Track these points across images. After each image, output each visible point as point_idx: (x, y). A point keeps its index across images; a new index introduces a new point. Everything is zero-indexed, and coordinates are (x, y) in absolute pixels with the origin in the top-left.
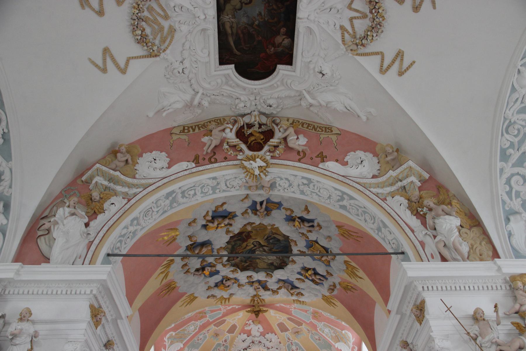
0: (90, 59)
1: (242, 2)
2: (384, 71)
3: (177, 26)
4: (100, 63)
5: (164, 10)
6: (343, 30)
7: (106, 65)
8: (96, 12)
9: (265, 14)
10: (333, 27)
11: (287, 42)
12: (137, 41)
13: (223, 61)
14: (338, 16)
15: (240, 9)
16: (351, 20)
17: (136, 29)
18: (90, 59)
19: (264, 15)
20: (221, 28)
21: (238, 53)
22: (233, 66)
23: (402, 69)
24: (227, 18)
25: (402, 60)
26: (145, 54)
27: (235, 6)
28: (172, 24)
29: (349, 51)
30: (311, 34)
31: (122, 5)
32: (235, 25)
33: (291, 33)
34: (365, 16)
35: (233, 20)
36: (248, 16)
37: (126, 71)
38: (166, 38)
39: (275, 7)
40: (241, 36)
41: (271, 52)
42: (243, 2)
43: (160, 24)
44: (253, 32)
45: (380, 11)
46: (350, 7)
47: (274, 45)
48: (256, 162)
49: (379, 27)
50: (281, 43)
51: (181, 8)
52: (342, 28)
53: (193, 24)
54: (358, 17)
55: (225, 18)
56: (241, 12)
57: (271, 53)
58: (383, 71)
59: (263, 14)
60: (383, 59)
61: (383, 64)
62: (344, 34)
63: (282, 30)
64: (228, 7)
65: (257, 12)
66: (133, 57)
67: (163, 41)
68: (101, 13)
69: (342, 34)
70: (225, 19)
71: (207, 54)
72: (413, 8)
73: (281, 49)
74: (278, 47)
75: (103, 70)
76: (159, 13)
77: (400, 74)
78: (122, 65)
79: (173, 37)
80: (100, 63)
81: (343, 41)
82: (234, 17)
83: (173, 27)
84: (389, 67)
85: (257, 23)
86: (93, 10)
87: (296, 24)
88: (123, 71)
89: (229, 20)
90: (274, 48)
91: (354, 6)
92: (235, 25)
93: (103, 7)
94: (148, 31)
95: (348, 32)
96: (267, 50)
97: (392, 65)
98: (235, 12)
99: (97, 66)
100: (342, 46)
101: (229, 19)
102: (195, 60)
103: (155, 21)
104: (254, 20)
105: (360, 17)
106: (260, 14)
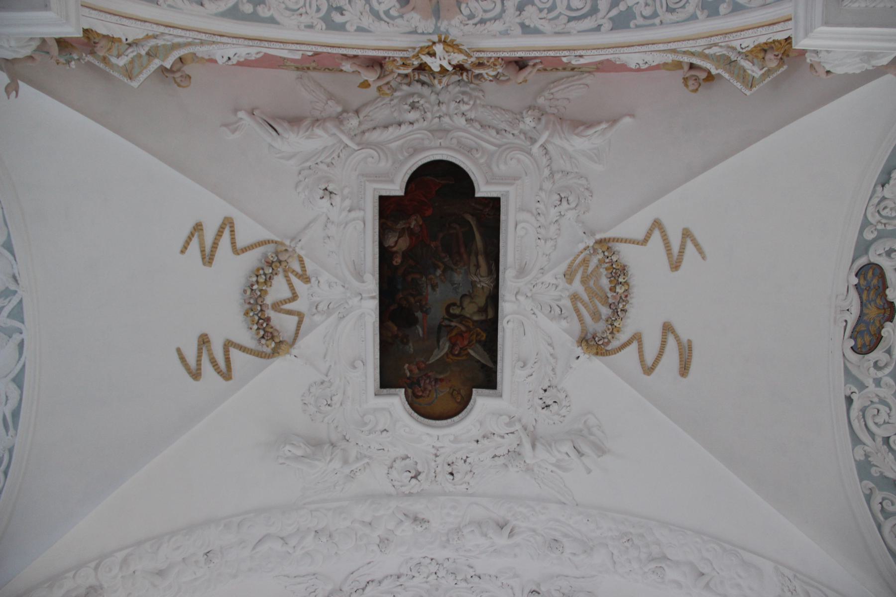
0: (704, 258)
1: (461, 308)
2: (226, 225)
3: (562, 283)
4: (690, 247)
5: (577, 311)
6: (305, 277)
7: (682, 242)
8: (673, 332)
9: (427, 287)
10: (321, 281)
11: (391, 241)
12: (625, 272)
13: (494, 204)
14: (316, 299)
15: (464, 296)
16: (294, 297)
17: (623, 296)
18: (704, 258)
19: (427, 285)
20: (493, 267)
21: (469, 218)
22: (477, 195)
23: (199, 236)
24: (484, 283)
25: (203, 251)
26: (617, 244)
27: (471, 302)
28: (568, 286)
29: (290, 250)
30: (354, 261)
31: (635, 334)
32: (473, 269)
33: (385, 254)
34: (276, 306)
35: (475, 279)
36: (453, 284)
37: (653, 224)
38: (579, 265)
39: (412, 300)
40: (463, 250)
41: (416, 220)
42: (458, 307)
43: (586, 290)
44: (443, 255)
45: (255, 327)
46: (300, 316)
47: (411, 233)
48: (441, 66)
49: (252, 301)
50: (399, 238)
51: (551, 311)
52: (305, 279)
53: (536, 284)
54: (286, 303)
55: (486, 283)
56: (462, 290)
57: (415, 217)
58: (228, 224)
59: (429, 288)
60: (232, 243)
61: (231, 235)
62: (302, 270)
63: (399, 261)
64: (481, 301)
65: (438, 290)
66: (638, 244)
67: (585, 261)
68: (668, 328)
69: (305, 271)
70: (487, 282)
71: (519, 227)
72: (209, 341)
73: (399, 225)
74: (403, 229)
75: (689, 235)
76: (585, 307)
77: (199, 227)
78: (657, 234)
79: (570, 266)
80: (690, 247)
81: (301, 261)
82: (473, 284)
83: (567, 282)
84: (220, 234)
85: (439, 272)
86: (677, 337)
87: (378, 281)
88: (657, 224)
89: (482, 279)
90: (409, 227)
91: (295, 319)
92: (473, 269)
93: (662, 338)
94: (605, 282)
95: (297, 275)
96: (421, 223)
97: (216, 239)
98: (471, 291)
99: (696, 245)
100: (302, 253)
101: (480, 281)
102: (539, 218)
103: (592, 294)
104: (443, 277)
105: (283, 304)
106: (434, 287)
